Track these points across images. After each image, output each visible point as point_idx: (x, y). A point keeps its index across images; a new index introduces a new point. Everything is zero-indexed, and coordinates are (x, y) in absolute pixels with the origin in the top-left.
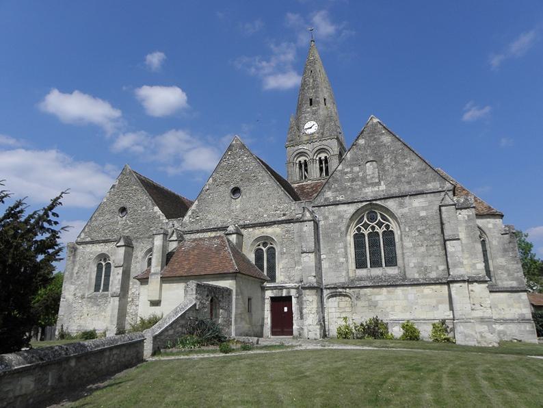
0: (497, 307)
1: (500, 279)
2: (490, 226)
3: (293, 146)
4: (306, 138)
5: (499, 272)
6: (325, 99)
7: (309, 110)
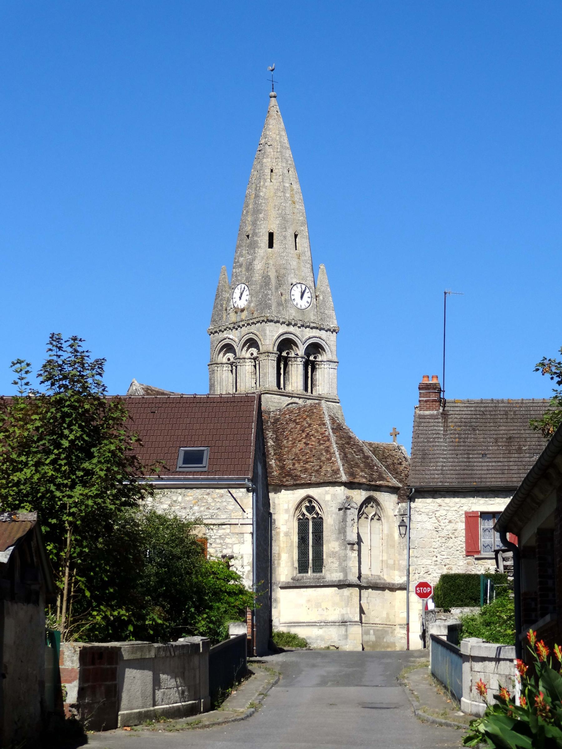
0: (320, 606)
1: (329, 570)
2: (328, 497)
3: (216, 332)
4: (233, 318)
5: (330, 560)
6: (271, 235)
7: (241, 259)
